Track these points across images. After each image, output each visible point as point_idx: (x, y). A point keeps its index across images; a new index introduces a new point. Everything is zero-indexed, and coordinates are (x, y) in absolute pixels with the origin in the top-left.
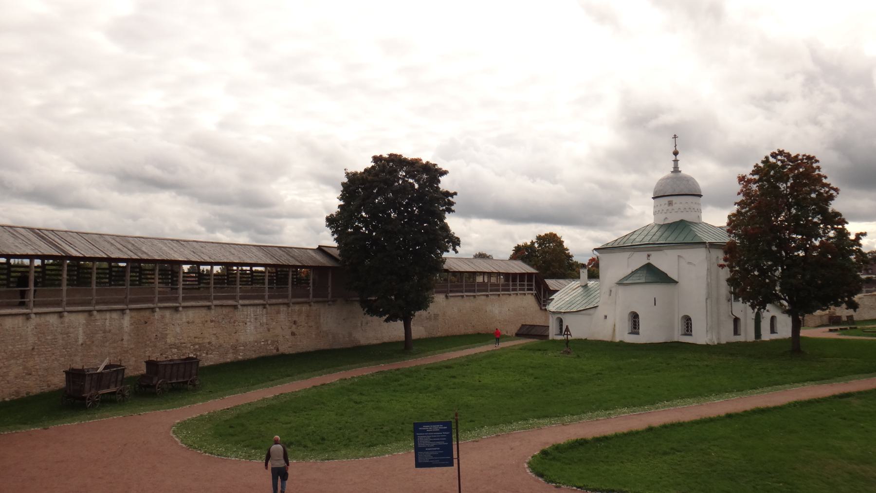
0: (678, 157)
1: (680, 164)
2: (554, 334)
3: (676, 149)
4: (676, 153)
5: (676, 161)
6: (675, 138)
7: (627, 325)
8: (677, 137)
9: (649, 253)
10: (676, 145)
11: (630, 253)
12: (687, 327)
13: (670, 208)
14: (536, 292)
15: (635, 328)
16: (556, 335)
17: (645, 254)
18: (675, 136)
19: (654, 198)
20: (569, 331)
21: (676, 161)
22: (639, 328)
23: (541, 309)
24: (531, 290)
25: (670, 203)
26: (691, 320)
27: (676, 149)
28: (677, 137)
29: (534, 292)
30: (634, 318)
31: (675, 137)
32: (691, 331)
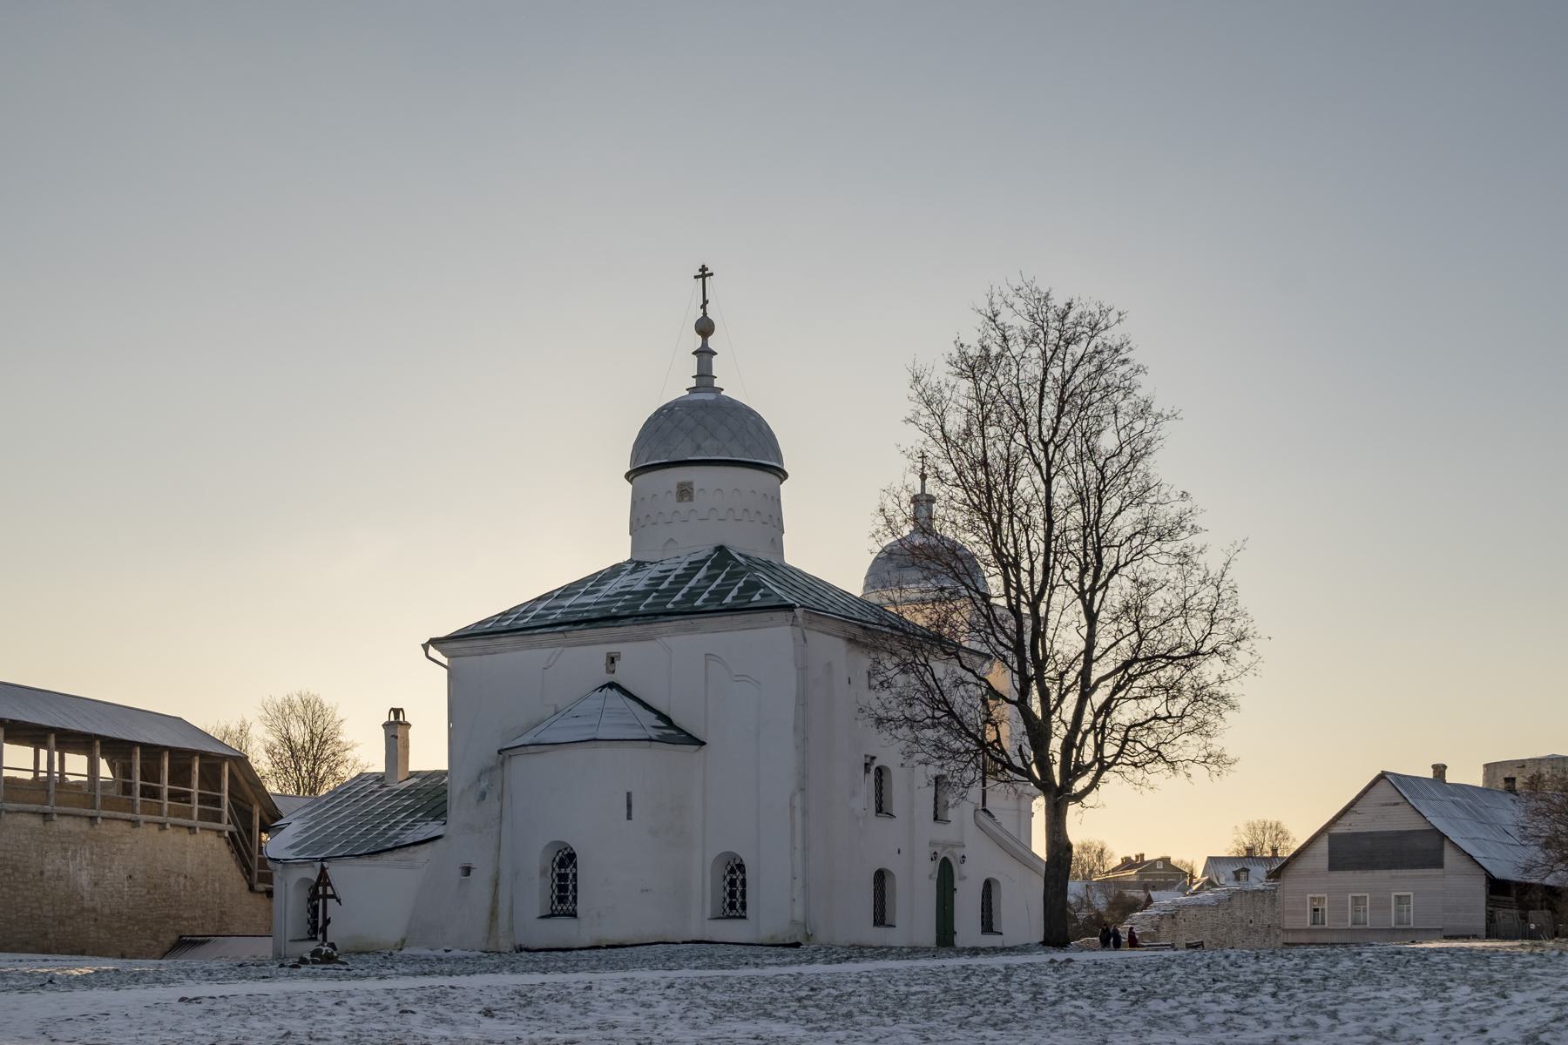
0: (713, 342)
2: (288, 938)
3: (705, 314)
4: (705, 328)
5: (705, 354)
6: (704, 276)
7: (535, 892)
8: (712, 274)
9: (613, 648)
10: (705, 302)
11: (553, 650)
12: (732, 894)
13: (684, 507)
14: (232, 828)
15: (562, 900)
16: (290, 941)
17: (600, 653)
18: (704, 269)
19: (630, 476)
20: (329, 884)
21: (705, 354)
22: (575, 898)
23: (251, 889)
24: (217, 818)
25: (685, 492)
26: (743, 872)
27: (705, 314)
28: (712, 274)
29: (226, 827)
30: (562, 864)
31: (704, 273)
32: (744, 906)
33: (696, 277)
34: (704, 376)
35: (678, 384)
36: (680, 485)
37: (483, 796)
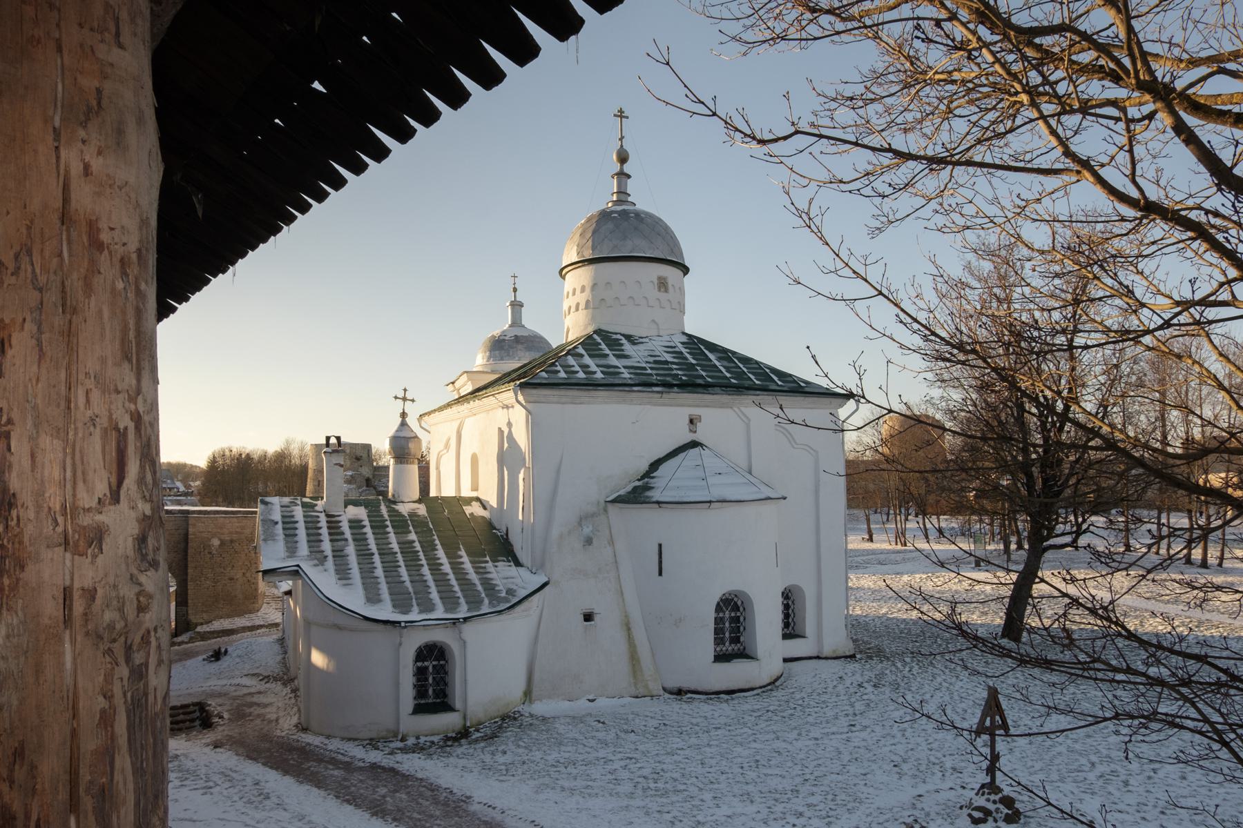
0: (627, 168)
1: (631, 187)
3: (622, 146)
4: (623, 158)
5: (622, 176)
8: (627, 117)
9: (695, 411)
13: (662, 296)
17: (685, 412)
18: (621, 111)
27: (622, 146)
28: (627, 117)
33: (615, 115)
34: (622, 192)
35: (604, 198)
36: (659, 278)
37: (589, 541)
